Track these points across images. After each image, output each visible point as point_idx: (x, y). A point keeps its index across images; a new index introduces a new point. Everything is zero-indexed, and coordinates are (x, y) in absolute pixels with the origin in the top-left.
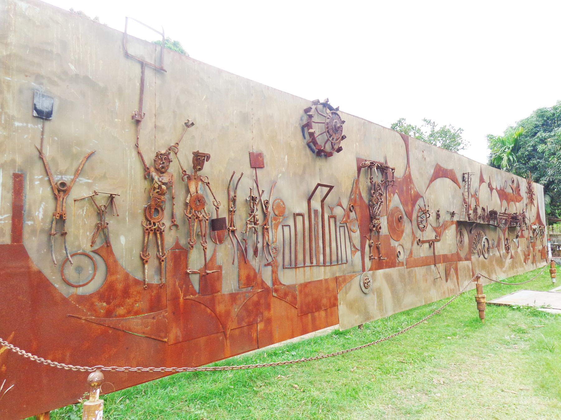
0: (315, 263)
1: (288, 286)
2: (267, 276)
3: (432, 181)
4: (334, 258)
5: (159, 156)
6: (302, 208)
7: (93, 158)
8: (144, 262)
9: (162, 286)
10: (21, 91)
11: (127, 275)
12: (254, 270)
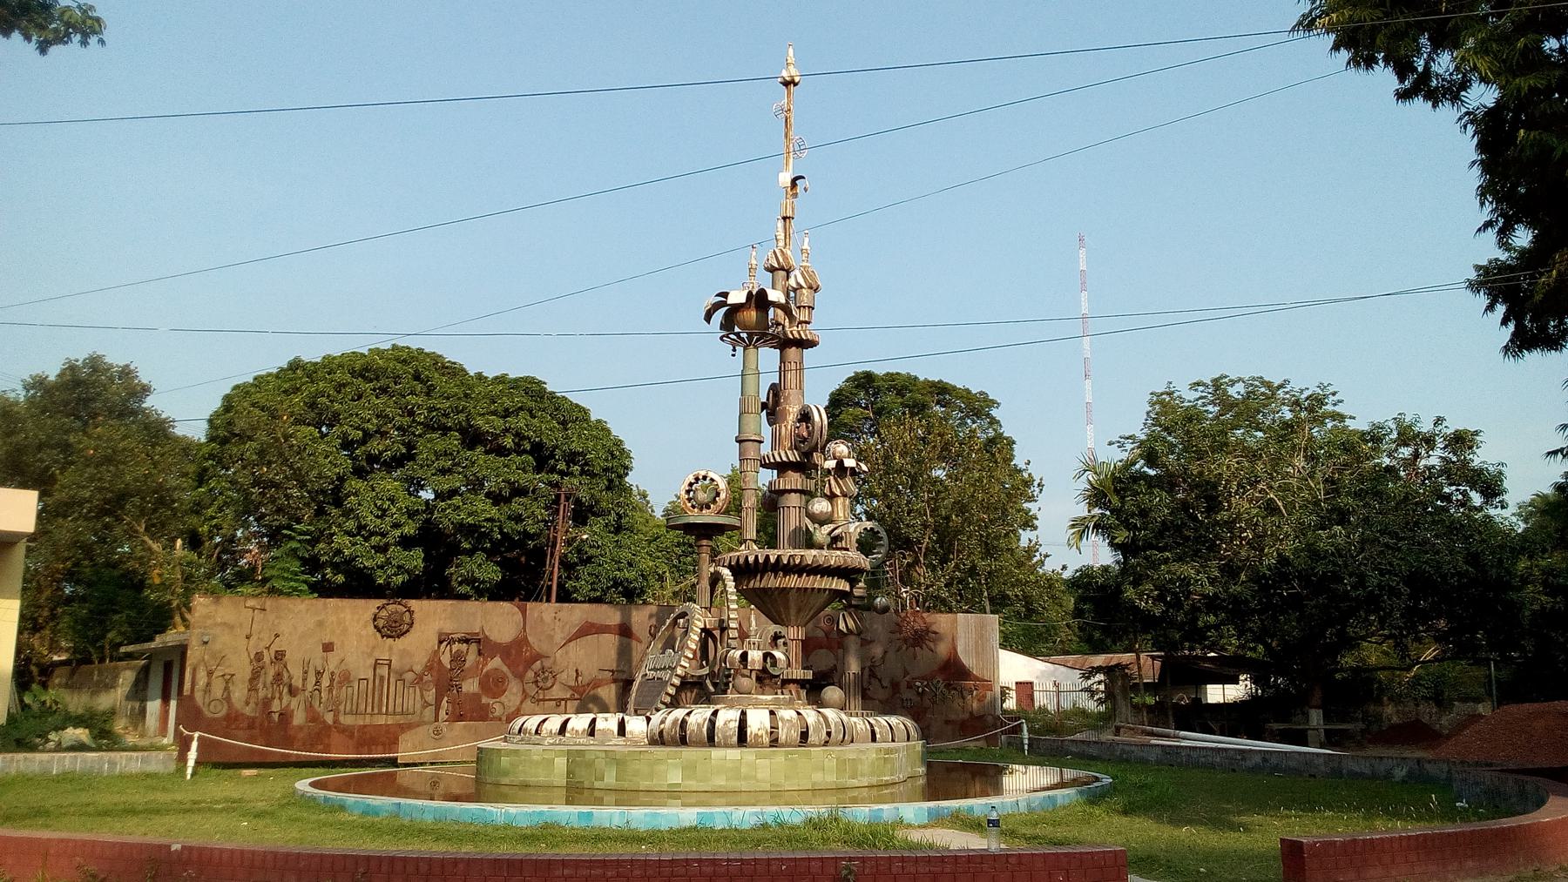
0: (376, 711)
1: (348, 726)
2: (329, 718)
3: (570, 640)
4: (399, 710)
6: (370, 675)
8: (247, 703)
10: (198, 634)
11: (237, 712)
12: (319, 714)
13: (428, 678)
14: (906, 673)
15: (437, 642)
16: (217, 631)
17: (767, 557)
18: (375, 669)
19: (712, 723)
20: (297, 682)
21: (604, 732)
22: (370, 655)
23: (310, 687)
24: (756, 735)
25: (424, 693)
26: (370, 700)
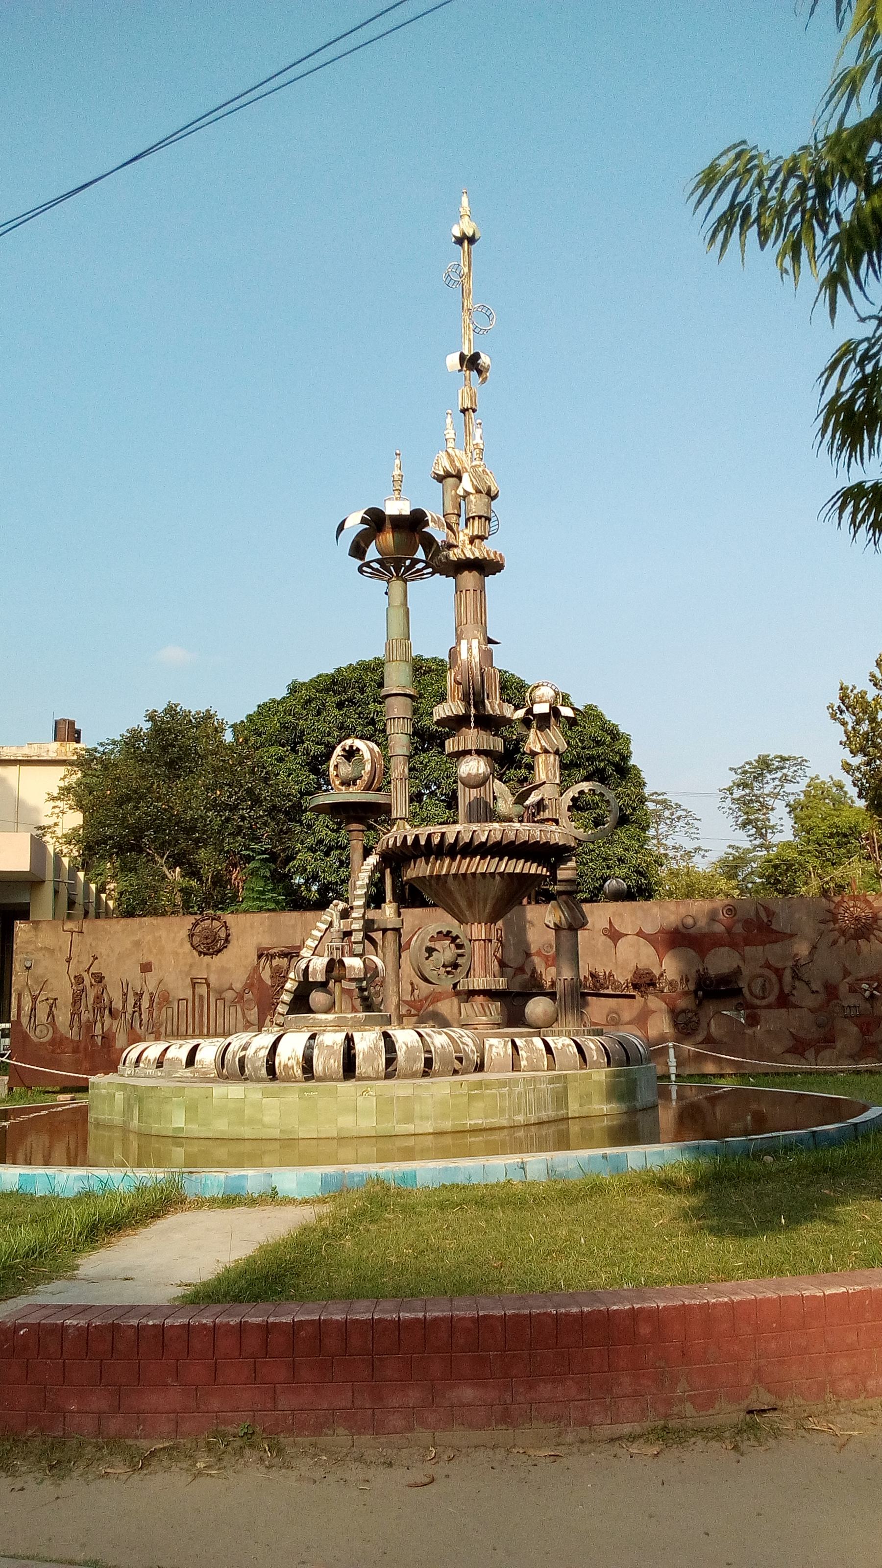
5: (75, 977)
7: (47, 983)
9: (79, 1041)
13: (248, 996)
14: (846, 973)
15: (256, 957)
16: (39, 955)
17: (417, 837)
18: (194, 988)
19: (274, 1049)
20: (118, 1005)
21: (174, 1061)
22: (188, 973)
23: (130, 1009)
24: (286, 1066)
25: (246, 1011)
26: (190, 1021)
